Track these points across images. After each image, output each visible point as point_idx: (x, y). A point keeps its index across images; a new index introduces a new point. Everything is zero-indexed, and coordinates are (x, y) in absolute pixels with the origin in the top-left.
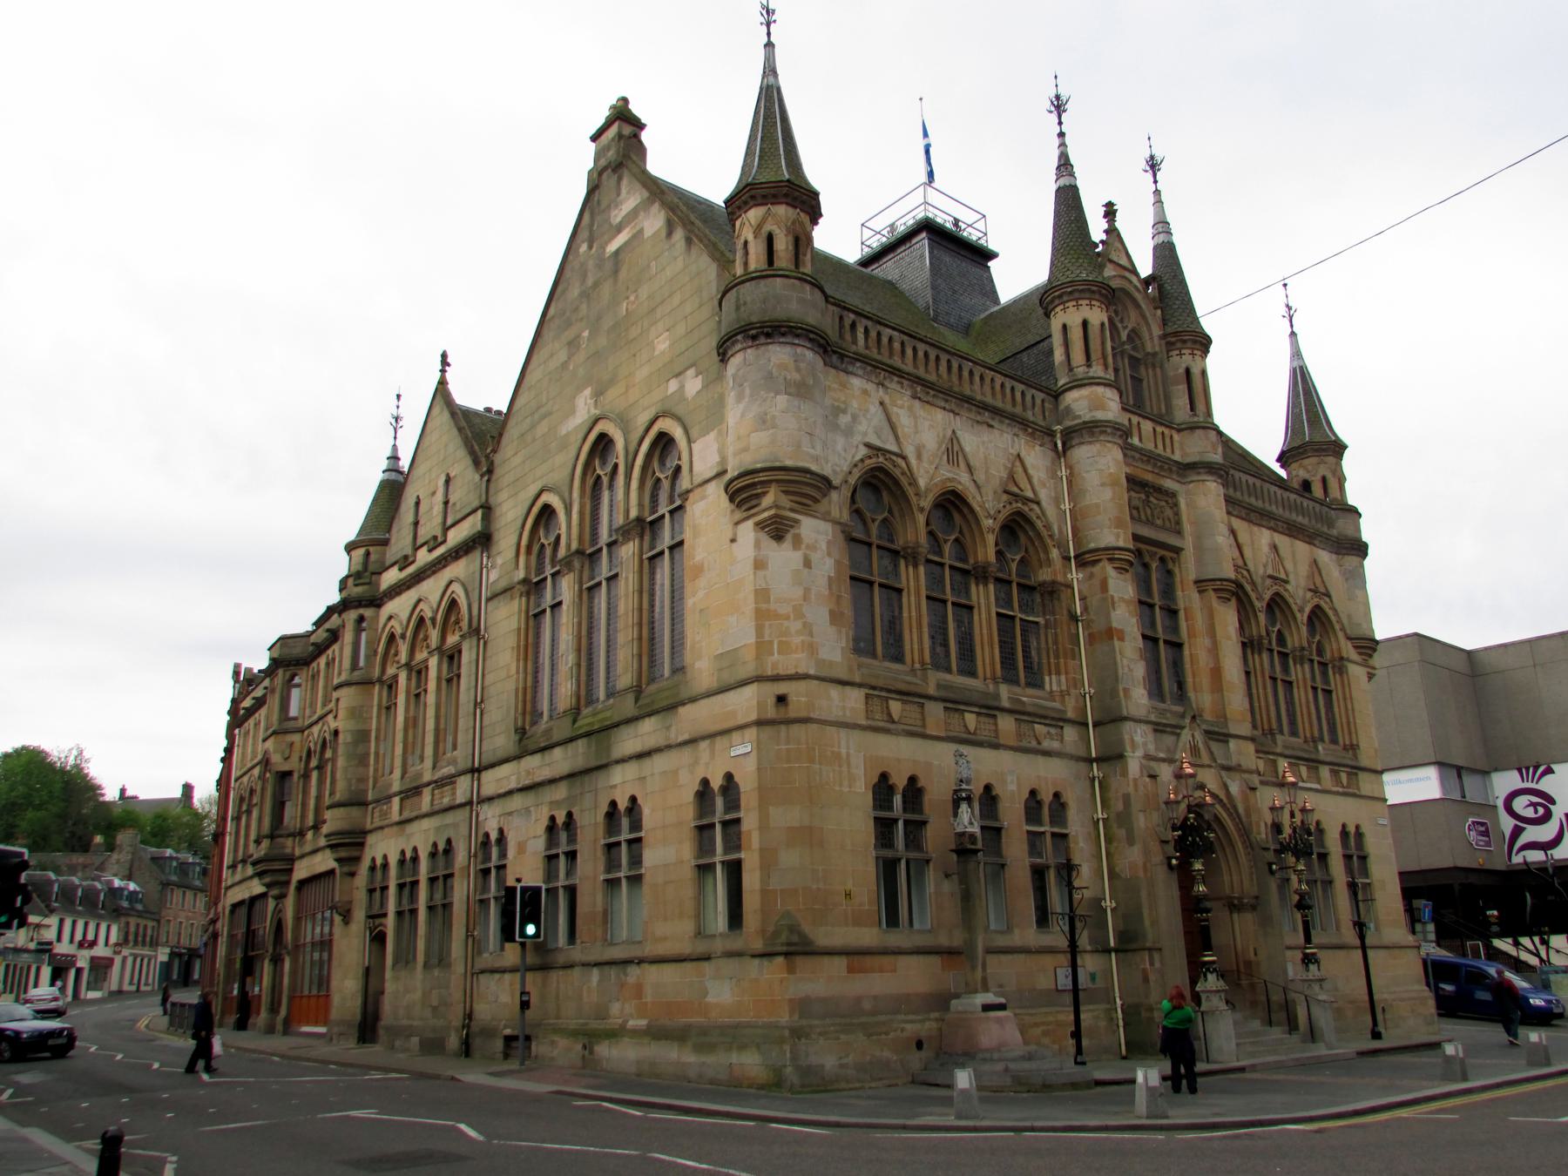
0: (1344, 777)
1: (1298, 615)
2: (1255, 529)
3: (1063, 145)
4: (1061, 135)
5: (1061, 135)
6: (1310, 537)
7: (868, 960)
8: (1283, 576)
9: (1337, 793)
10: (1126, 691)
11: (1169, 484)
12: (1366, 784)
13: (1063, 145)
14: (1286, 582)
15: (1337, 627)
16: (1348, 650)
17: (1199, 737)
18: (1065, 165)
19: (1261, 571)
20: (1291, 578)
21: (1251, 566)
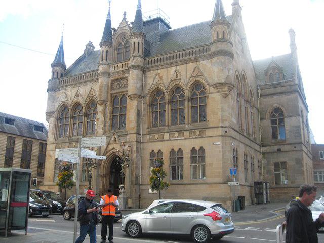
0: (198, 133)
1: (185, 88)
2: (169, 69)
3: (109, 10)
4: (109, 8)
5: (109, 8)
6: (196, 60)
7: (51, 187)
8: (179, 78)
9: (195, 138)
10: (97, 132)
11: (126, 76)
12: (209, 133)
13: (109, 10)
14: (180, 79)
15: (206, 84)
16: (212, 89)
17: (116, 136)
18: (109, 14)
19: (169, 80)
20: (184, 77)
21: (165, 81)
